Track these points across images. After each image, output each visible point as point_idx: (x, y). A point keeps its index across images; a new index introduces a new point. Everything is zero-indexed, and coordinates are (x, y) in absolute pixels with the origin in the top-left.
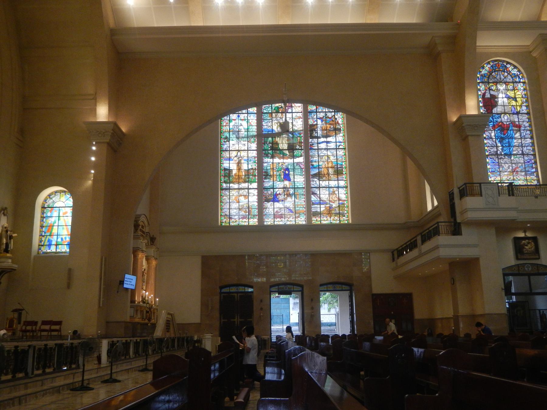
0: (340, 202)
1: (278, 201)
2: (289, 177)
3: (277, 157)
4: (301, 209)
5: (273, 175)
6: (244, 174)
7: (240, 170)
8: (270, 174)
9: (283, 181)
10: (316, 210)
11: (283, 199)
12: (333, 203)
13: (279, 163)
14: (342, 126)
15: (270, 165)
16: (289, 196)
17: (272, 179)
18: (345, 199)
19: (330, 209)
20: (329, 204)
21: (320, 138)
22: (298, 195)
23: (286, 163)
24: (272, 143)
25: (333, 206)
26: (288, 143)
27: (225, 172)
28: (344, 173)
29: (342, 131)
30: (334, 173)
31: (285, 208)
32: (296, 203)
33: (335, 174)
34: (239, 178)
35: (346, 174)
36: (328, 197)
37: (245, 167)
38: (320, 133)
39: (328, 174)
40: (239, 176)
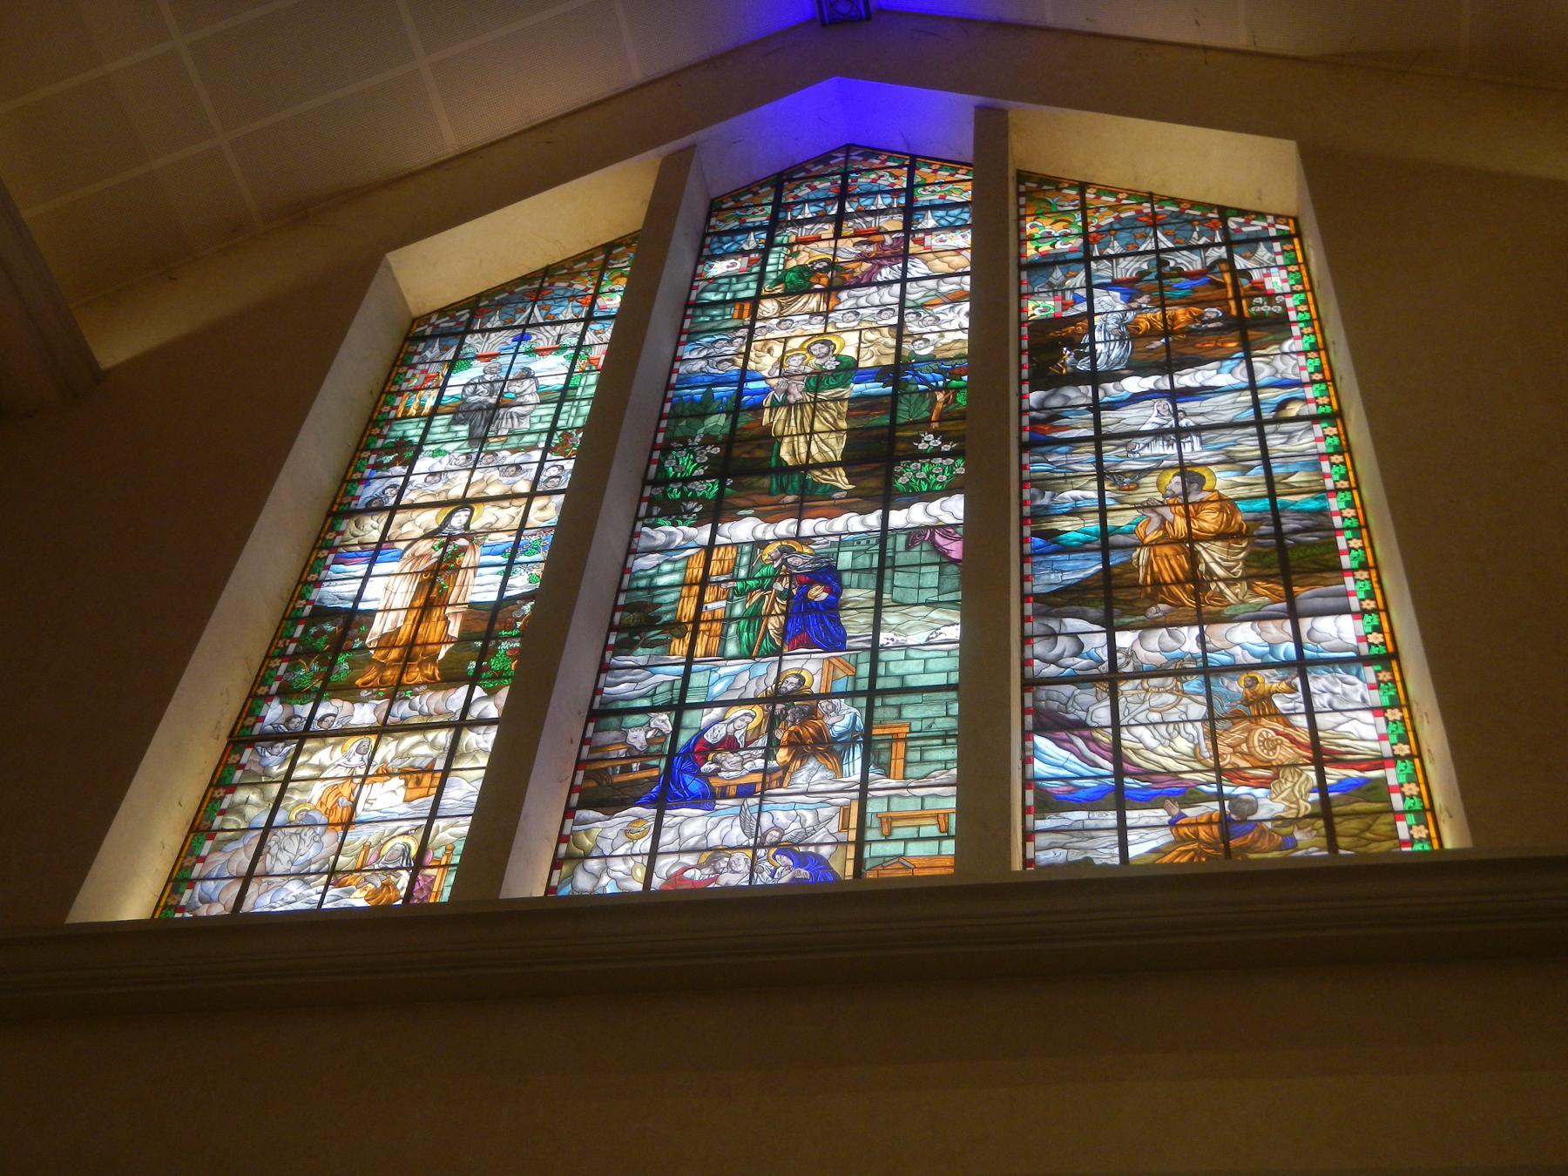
0: (1334, 775)
1: (706, 799)
2: (836, 621)
3: (750, 512)
4: (915, 849)
5: (697, 620)
6: (454, 630)
7: (436, 613)
8: (668, 617)
9: (779, 652)
10: (1075, 856)
11: (757, 778)
12: (1264, 783)
13: (761, 544)
14: (1290, 302)
15: (679, 565)
16: (814, 754)
17: (680, 648)
18: (1386, 748)
19: (1226, 836)
20: (1220, 797)
21: (1115, 377)
22: (901, 746)
23: (818, 540)
24: (730, 440)
25: (1262, 814)
26: (848, 431)
27: (313, 630)
28: (1346, 561)
29: (1295, 330)
30: (1254, 571)
31: (761, 852)
32: (873, 807)
33: (1266, 578)
34: (407, 660)
35: (1364, 566)
36: (1205, 745)
37: (481, 586)
38: (1108, 351)
39: (1197, 580)
40: (411, 643)
